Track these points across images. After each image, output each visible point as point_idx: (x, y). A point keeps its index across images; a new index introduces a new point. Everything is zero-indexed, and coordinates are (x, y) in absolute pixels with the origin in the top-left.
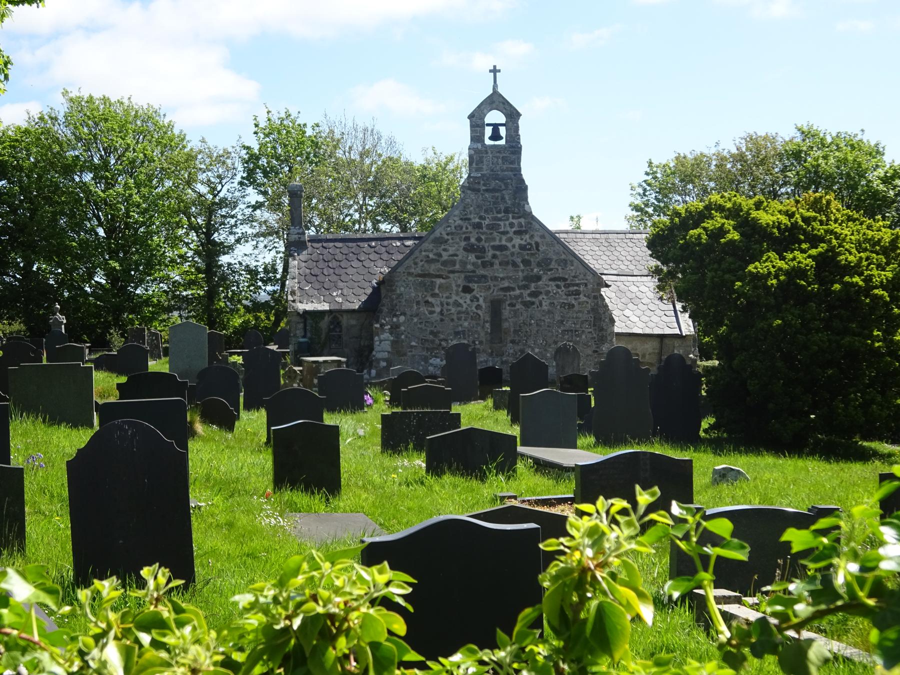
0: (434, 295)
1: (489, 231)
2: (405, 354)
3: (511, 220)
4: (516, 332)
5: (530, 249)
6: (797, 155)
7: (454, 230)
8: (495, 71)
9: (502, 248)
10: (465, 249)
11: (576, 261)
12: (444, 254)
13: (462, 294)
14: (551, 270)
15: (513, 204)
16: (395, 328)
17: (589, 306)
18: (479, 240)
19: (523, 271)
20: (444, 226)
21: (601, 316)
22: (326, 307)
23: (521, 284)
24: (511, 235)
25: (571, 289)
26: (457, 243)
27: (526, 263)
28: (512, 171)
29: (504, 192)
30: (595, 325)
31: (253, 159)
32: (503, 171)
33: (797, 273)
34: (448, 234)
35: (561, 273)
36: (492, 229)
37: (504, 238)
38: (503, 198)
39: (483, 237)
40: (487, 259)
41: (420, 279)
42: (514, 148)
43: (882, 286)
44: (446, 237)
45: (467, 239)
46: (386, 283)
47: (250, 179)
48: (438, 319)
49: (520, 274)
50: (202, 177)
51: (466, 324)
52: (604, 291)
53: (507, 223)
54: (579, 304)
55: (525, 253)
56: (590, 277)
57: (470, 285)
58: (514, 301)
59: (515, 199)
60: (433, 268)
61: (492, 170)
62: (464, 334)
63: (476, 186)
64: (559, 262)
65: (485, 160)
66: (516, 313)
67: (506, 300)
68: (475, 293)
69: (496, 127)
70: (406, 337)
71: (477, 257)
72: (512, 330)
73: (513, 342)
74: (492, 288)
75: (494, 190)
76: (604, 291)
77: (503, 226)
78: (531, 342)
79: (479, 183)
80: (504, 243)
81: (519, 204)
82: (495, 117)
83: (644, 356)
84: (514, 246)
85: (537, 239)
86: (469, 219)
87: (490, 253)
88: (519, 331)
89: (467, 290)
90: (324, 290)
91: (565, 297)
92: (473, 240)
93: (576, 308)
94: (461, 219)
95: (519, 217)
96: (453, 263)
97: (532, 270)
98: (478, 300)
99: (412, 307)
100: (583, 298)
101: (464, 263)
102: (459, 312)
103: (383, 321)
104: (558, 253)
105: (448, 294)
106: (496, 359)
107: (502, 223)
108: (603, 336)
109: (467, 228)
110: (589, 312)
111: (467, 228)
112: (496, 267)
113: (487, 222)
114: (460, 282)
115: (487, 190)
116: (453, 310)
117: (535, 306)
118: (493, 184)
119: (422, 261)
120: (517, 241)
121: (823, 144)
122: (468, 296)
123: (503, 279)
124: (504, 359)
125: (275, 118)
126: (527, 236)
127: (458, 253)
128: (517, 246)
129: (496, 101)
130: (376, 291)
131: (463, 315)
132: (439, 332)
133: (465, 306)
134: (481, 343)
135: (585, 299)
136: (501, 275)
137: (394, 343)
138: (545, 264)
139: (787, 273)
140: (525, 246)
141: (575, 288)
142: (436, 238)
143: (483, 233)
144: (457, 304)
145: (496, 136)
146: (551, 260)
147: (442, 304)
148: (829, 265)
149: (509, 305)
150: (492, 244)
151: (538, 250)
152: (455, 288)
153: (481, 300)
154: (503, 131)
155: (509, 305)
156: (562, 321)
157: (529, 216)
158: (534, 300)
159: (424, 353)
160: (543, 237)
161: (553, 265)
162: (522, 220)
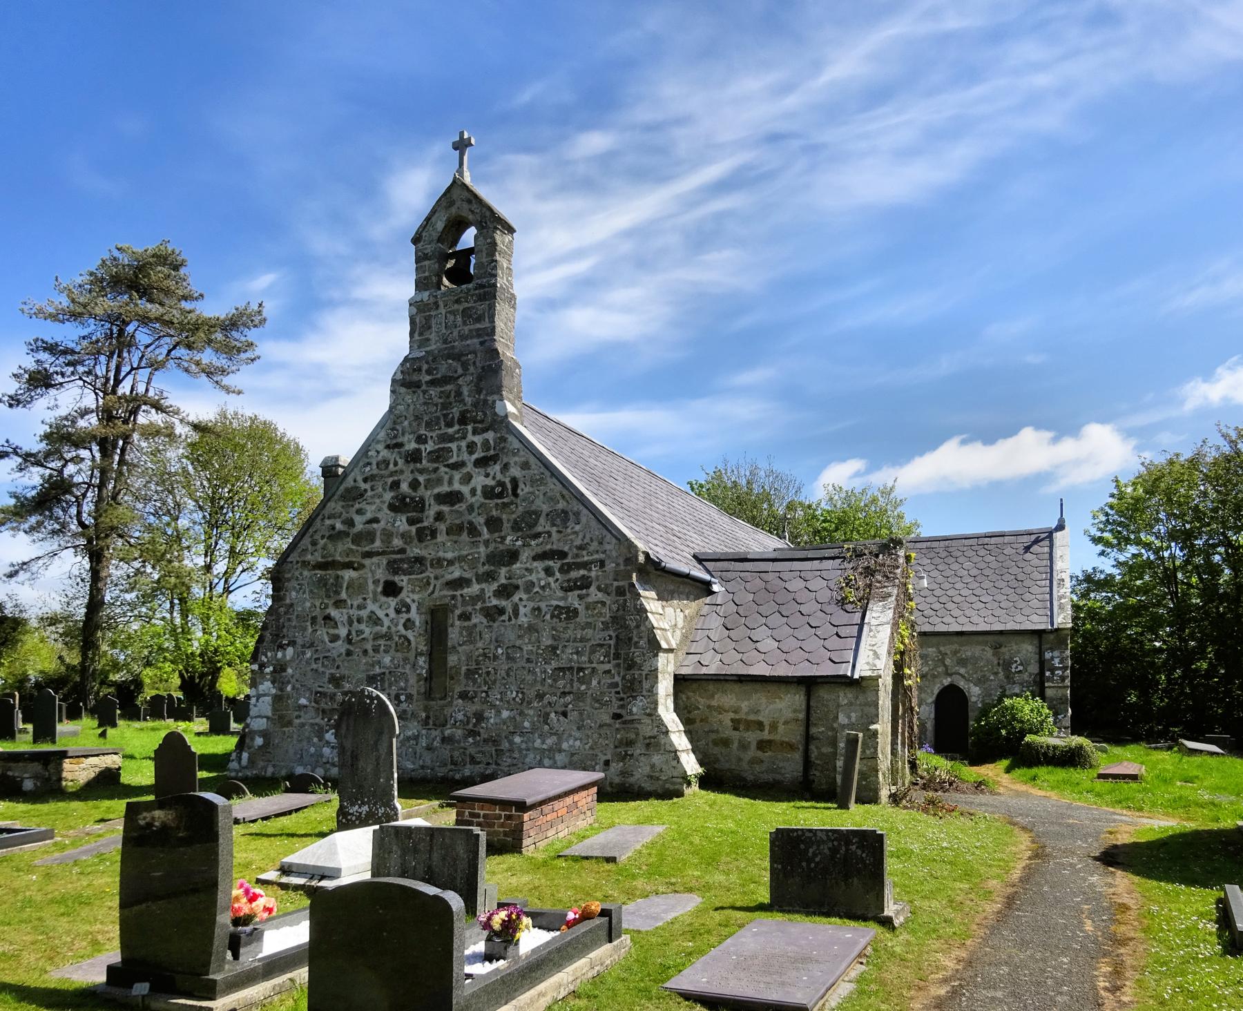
0: (339, 604)
1: (431, 466)
2: (290, 723)
3: (470, 437)
4: (470, 674)
5: (500, 496)
7: (375, 472)
9: (453, 498)
10: (392, 507)
11: (585, 511)
12: (359, 520)
13: (384, 599)
14: (537, 536)
15: (475, 405)
17: (605, 610)
18: (414, 485)
19: (487, 543)
20: (361, 464)
23: (481, 570)
24: (470, 468)
25: (574, 574)
26: (380, 496)
27: (494, 524)
28: (479, 336)
29: (460, 381)
30: (617, 656)
32: (463, 337)
34: (365, 480)
35: (556, 544)
36: (437, 460)
37: (457, 476)
38: (459, 394)
39: (421, 479)
40: (425, 524)
41: (319, 573)
44: (363, 486)
45: (395, 485)
48: (343, 651)
49: (482, 549)
51: (387, 660)
53: (463, 444)
54: (587, 608)
55: (492, 503)
56: (610, 545)
57: (396, 579)
58: (470, 609)
59: (479, 391)
60: (339, 551)
61: (445, 342)
62: (382, 680)
63: (415, 377)
64: (552, 516)
65: (433, 322)
66: (471, 635)
67: (455, 606)
68: (403, 595)
70: (293, 688)
71: (411, 522)
72: (464, 668)
73: (464, 696)
74: (433, 581)
75: (446, 380)
77: (457, 452)
78: (495, 696)
79: (420, 370)
80: (457, 486)
81: (485, 401)
83: (774, 727)
84: (473, 492)
85: (515, 472)
86: (400, 445)
87: (433, 509)
88: (476, 671)
89: (391, 589)
91: (560, 594)
92: (404, 487)
93: (582, 619)
94: (388, 447)
95: (485, 430)
96: (369, 536)
97: (503, 538)
98: (408, 611)
99: (305, 629)
100: (594, 594)
102: (377, 637)
103: (263, 658)
104: (551, 499)
105: (360, 601)
106: (434, 733)
107: (453, 446)
108: (633, 681)
109: (396, 464)
110: (606, 626)
111: (396, 464)
112: (441, 538)
113: (430, 446)
114: (382, 574)
115: (432, 383)
116: (367, 631)
117: (505, 617)
118: (443, 368)
119: (323, 537)
120: (479, 481)
122: (393, 602)
123: (451, 563)
124: (447, 732)
126: (497, 467)
127: (379, 515)
128: (479, 492)
131: (382, 642)
132: (342, 678)
133: (386, 622)
134: (409, 697)
135: (600, 595)
136: (449, 555)
137: (277, 699)
138: (526, 525)
140: (493, 488)
141: (582, 572)
142: (348, 490)
143: (421, 472)
144: (375, 620)
146: (538, 514)
147: (350, 622)
149: (460, 617)
150: (436, 491)
151: (515, 495)
152: (371, 587)
153: (414, 607)
155: (460, 617)
156: (554, 648)
157: (501, 424)
158: (504, 603)
159: (318, 720)
160: (525, 466)
161: (543, 525)
162: (490, 435)
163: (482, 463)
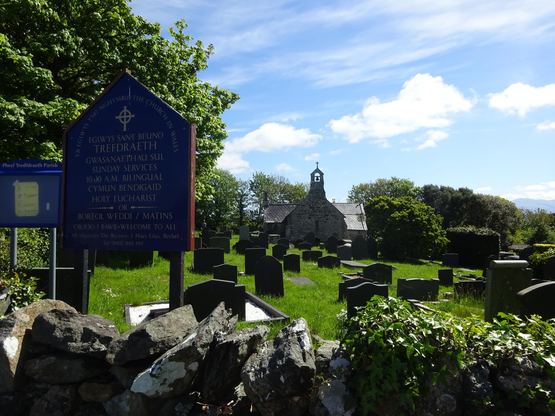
6: (391, 184)
8: (317, 163)
9: (319, 207)
16: (291, 227)
21: (344, 225)
22: (273, 222)
27: (325, 211)
31: (252, 183)
33: (403, 217)
42: (322, 182)
43: (425, 220)
46: (289, 216)
47: (251, 189)
50: (240, 188)
52: (345, 219)
60: (301, 212)
69: (317, 177)
76: (345, 219)
82: (317, 174)
87: (316, 209)
89: (310, 218)
90: (273, 217)
101: (309, 211)
114: (308, 216)
120: (323, 206)
121: (398, 181)
125: (258, 173)
129: (317, 170)
130: (286, 218)
137: (291, 231)
138: (330, 212)
139: (401, 217)
144: (307, 222)
145: (317, 179)
148: (412, 215)
154: (319, 178)
157: (326, 199)
163: (323, 204)
